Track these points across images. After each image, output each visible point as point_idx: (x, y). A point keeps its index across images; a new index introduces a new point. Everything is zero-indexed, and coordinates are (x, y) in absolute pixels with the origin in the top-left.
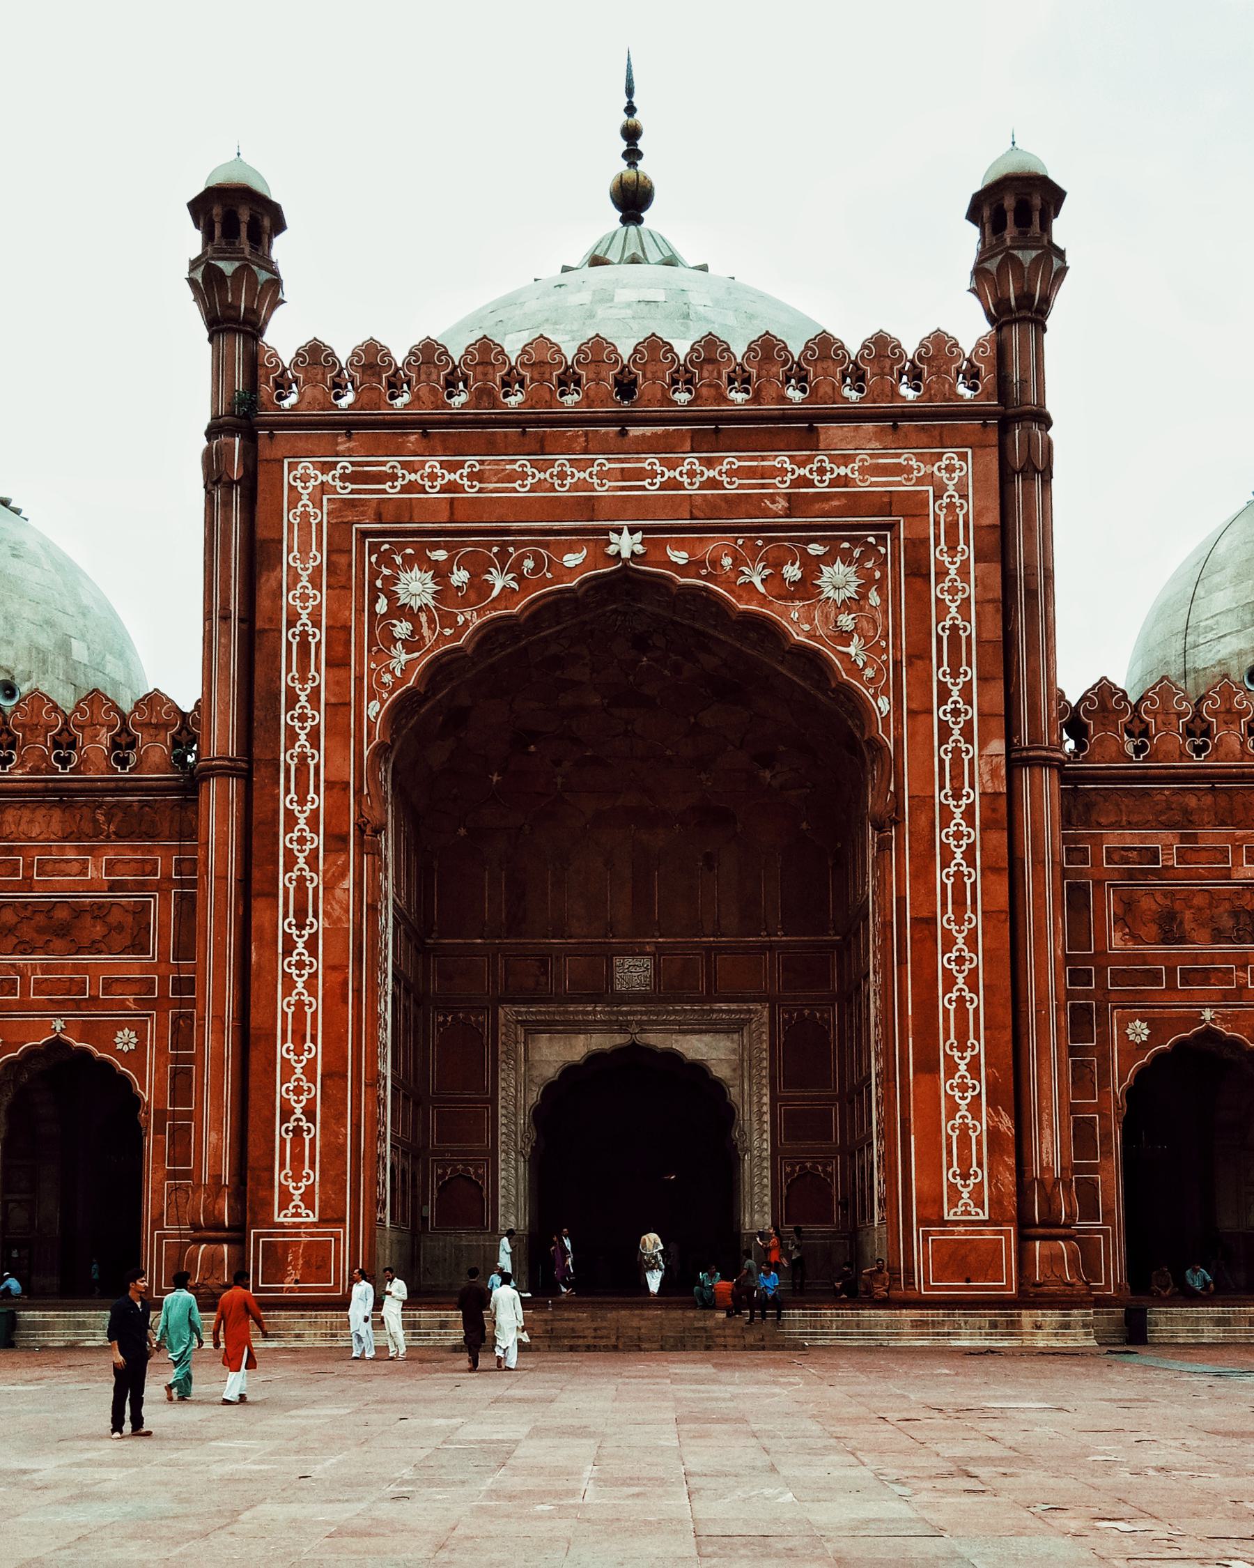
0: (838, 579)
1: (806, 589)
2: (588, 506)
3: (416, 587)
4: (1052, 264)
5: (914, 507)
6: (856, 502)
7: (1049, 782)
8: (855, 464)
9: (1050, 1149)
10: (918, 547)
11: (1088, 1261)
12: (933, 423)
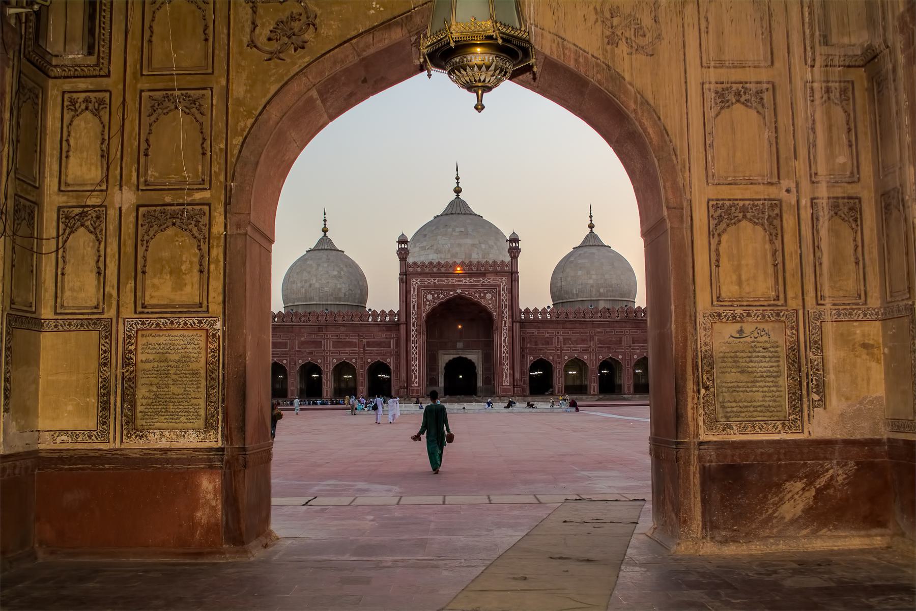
0: (489, 296)
1: (484, 297)
2: (454, 286)
3: (430, 297)
4: (518, 250)
5: (499, 286)
6: (491, 285)
7: (518, 325)
8: (490, 280)
9: (517, 376)
10: (500, 292)
11: (523, 390)
12: (502, 274)
